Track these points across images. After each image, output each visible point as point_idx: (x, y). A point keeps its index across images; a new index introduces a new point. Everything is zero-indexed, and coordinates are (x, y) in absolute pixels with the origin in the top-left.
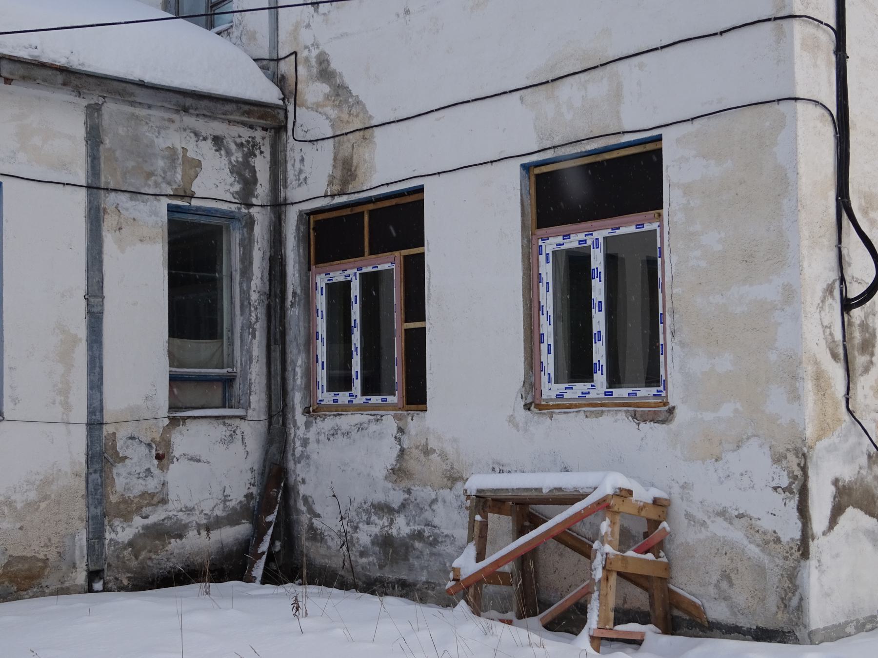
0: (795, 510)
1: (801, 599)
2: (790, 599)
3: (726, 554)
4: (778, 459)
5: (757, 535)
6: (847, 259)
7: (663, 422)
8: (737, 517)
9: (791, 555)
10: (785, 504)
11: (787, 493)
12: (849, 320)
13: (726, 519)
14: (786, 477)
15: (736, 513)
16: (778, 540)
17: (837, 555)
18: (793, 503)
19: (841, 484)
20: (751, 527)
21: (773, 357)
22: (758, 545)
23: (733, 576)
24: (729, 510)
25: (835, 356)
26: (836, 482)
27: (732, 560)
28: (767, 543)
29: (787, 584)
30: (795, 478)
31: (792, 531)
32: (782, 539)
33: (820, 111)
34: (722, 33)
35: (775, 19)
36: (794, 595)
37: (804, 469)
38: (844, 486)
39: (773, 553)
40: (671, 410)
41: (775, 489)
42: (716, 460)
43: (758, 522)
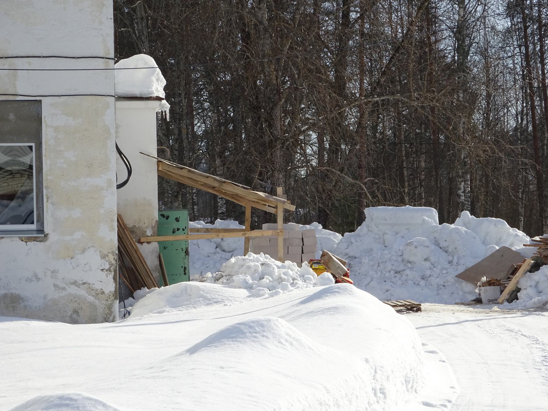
2: (109, 318)
3: (76, 301)
4: (104, 257)
5: (93, 291)
7: (41, 241)
8: (82, 284)
9: (110, 298)
10: (107, 277)
11: (108, 272)
13: (76, 286)
14: (108, 264)
15: (82, 282)
16: (103, 293)
21: (102, 211)
22: (93, 296)
23: (79, 311)
24: (78, 281)
27: (79, 304)
28: (97, 294)
29: (107, 311)
30: (112, 265)
32: (105, 292)
36: (110, 315)
39: (100, 299)
40: (46, 236)
41: (102, 270)
42: (71, 259)
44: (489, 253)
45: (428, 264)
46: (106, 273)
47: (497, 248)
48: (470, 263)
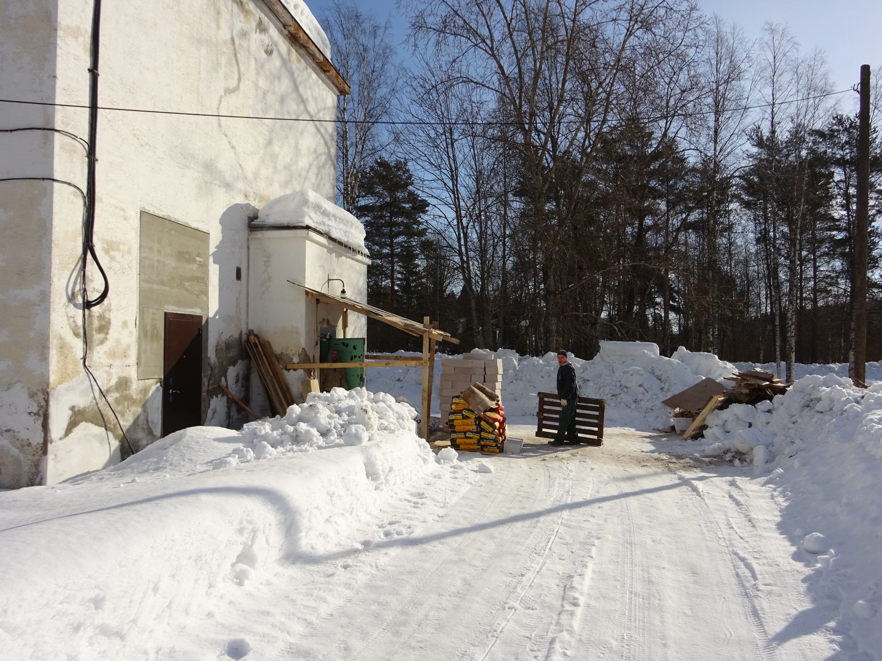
0: (41, 426)
1: (42, 479)
2: (35, 479)
4: (32, 396)
6: (90, 278)
8: (6, 431)
12: (89, 314)
15: (6, 429)
16: (29, 445)
17: (71, 451)
18: (40, 422)
19: (76, 409)
20: (14, 437)
21: (32, 334)
22: (18, 448)
25: (76, 335)
26: (72, 408)
28: (23, 446)
29: (34, 470)
30: (42, 407)
31: (38, 439)
33: (72, 188)
34: (11, 131)
35: (44, 129)
37: (47, 401)
38: (79, 410)
41: (30, 413)
43: (19, 434)
44: (696, 382)
45: (641, 389)
46: (34, 417)
47: (704, 378)
48: (678, 389)
